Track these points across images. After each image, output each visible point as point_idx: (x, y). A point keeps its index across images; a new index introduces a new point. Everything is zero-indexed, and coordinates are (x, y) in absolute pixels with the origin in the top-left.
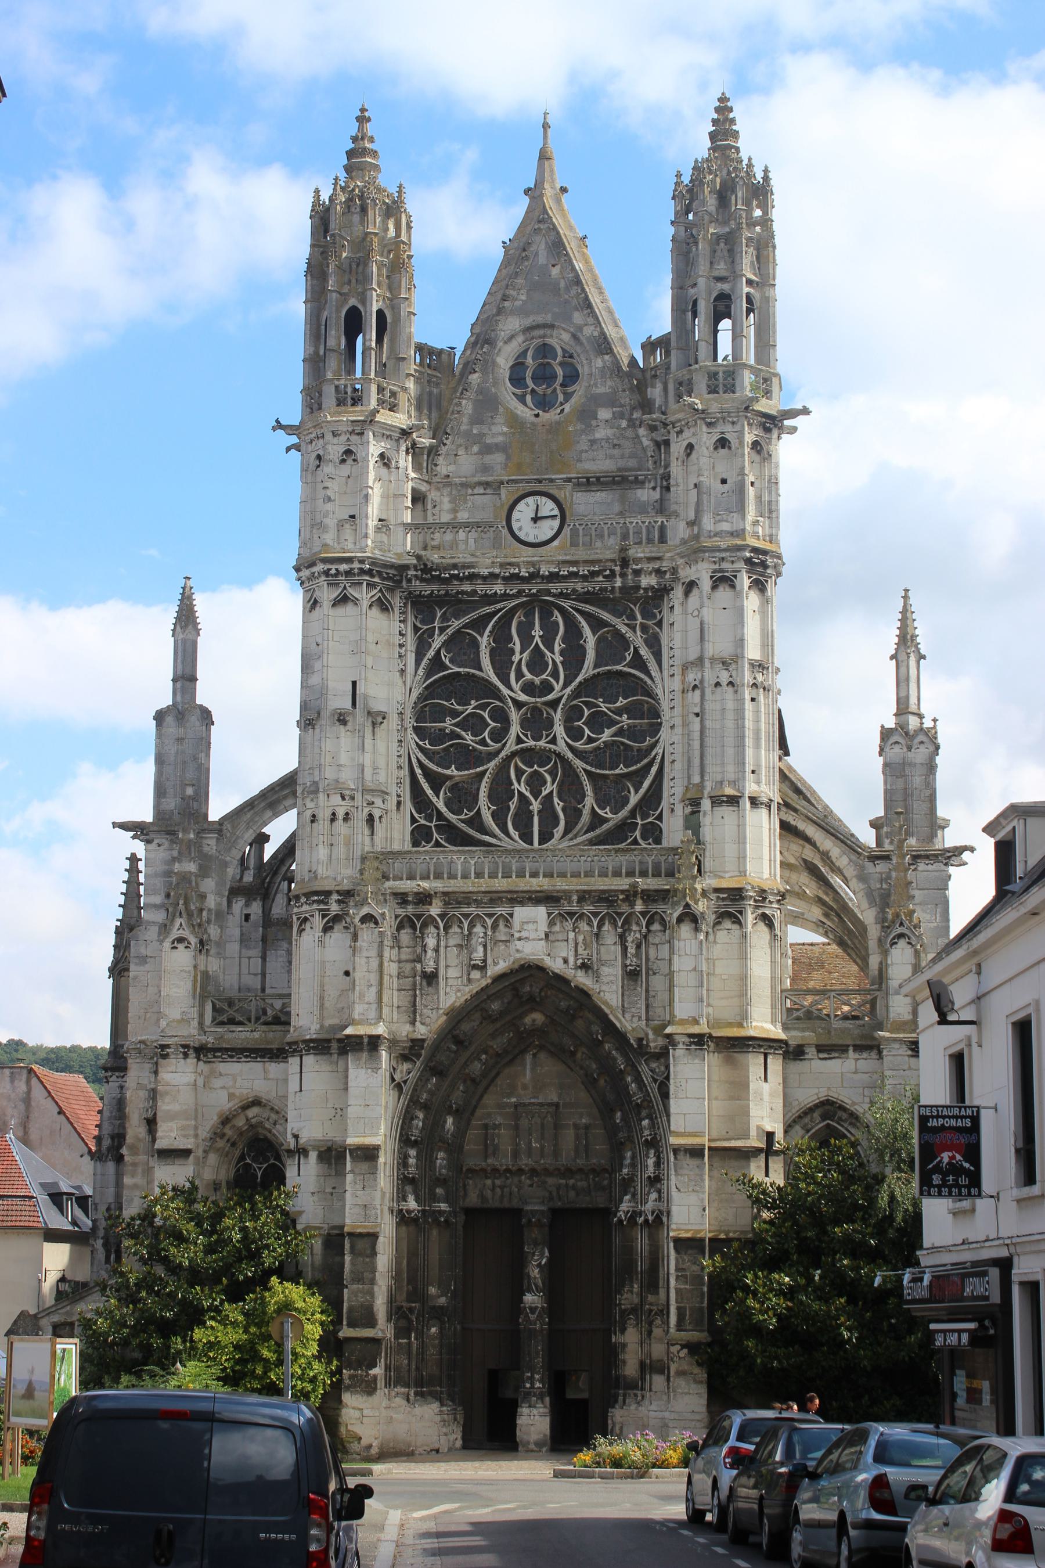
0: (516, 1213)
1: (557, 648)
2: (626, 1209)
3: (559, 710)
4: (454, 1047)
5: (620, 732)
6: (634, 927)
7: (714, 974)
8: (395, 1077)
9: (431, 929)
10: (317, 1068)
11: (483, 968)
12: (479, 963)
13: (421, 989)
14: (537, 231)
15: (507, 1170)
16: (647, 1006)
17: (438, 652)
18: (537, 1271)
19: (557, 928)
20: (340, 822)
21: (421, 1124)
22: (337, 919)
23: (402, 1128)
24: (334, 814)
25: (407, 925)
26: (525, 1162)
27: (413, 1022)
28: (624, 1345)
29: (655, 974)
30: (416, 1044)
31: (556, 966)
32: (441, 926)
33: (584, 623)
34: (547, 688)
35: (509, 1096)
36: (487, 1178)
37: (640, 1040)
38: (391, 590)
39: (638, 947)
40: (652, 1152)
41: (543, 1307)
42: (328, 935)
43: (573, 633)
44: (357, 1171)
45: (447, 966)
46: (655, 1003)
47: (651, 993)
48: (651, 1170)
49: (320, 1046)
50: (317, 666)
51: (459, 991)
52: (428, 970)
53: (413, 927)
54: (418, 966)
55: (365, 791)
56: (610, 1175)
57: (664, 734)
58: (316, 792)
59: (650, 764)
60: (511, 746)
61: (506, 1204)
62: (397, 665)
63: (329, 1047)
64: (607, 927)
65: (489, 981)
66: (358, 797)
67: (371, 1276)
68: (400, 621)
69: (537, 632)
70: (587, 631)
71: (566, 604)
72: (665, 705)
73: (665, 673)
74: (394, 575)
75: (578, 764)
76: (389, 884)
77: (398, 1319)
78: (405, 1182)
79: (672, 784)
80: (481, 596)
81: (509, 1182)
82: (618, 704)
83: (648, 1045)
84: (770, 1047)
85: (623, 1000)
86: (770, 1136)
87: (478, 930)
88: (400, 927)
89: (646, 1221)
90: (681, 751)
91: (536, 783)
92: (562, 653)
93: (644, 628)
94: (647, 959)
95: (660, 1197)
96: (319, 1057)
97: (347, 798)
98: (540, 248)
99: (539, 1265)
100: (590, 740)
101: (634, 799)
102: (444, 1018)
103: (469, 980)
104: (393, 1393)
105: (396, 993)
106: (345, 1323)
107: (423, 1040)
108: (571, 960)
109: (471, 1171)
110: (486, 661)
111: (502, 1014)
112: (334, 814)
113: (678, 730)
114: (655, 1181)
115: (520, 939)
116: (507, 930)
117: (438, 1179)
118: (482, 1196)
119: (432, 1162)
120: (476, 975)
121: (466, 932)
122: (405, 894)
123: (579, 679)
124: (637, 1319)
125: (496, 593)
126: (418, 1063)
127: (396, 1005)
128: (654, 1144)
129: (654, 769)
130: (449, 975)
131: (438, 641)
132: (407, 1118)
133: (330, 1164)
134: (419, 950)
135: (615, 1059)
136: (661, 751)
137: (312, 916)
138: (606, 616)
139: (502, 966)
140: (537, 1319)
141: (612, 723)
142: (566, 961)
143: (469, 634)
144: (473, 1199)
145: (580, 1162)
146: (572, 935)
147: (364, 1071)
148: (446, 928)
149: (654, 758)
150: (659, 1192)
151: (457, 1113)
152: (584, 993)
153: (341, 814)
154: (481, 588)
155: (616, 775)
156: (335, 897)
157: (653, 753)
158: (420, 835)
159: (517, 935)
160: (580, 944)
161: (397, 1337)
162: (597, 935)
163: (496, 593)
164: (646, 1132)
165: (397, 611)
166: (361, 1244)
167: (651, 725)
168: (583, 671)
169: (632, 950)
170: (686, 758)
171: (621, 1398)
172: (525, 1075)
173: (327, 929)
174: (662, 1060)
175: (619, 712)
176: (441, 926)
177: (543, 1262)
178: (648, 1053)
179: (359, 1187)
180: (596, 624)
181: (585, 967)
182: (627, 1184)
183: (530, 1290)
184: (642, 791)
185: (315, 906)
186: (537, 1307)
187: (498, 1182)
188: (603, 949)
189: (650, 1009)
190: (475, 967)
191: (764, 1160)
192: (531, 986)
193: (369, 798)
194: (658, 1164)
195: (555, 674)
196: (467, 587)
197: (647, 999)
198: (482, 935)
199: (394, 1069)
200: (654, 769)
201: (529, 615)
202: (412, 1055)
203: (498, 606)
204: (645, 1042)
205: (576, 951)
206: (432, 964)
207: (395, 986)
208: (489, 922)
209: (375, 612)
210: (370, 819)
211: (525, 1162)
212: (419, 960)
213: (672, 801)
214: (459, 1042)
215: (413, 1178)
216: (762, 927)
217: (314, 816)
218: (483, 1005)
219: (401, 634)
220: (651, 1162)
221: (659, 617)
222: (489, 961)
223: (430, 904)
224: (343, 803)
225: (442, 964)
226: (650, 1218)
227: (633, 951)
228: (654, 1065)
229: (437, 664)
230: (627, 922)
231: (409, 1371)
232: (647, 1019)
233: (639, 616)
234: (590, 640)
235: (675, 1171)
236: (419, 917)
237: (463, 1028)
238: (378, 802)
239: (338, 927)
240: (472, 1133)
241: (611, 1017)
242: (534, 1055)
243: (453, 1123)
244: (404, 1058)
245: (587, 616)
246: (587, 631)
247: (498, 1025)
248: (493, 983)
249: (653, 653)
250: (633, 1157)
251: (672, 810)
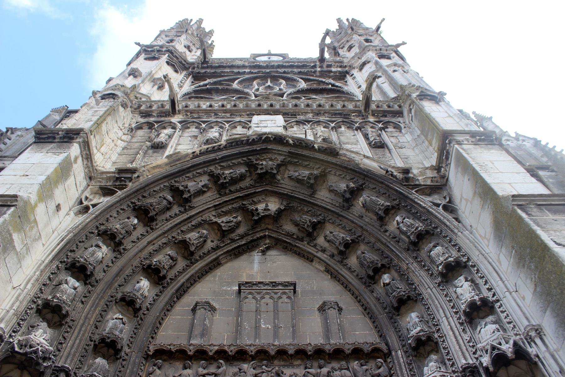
15: (222, 354)
35: (230, 284)
36: (185, 368)
37: (406, 171)
145: (336, 341)
172: (252, 268)
202: (115, 186)
226: (507, 348)
235: (538, 225)
242: (264, 252)
244: (106, 191)
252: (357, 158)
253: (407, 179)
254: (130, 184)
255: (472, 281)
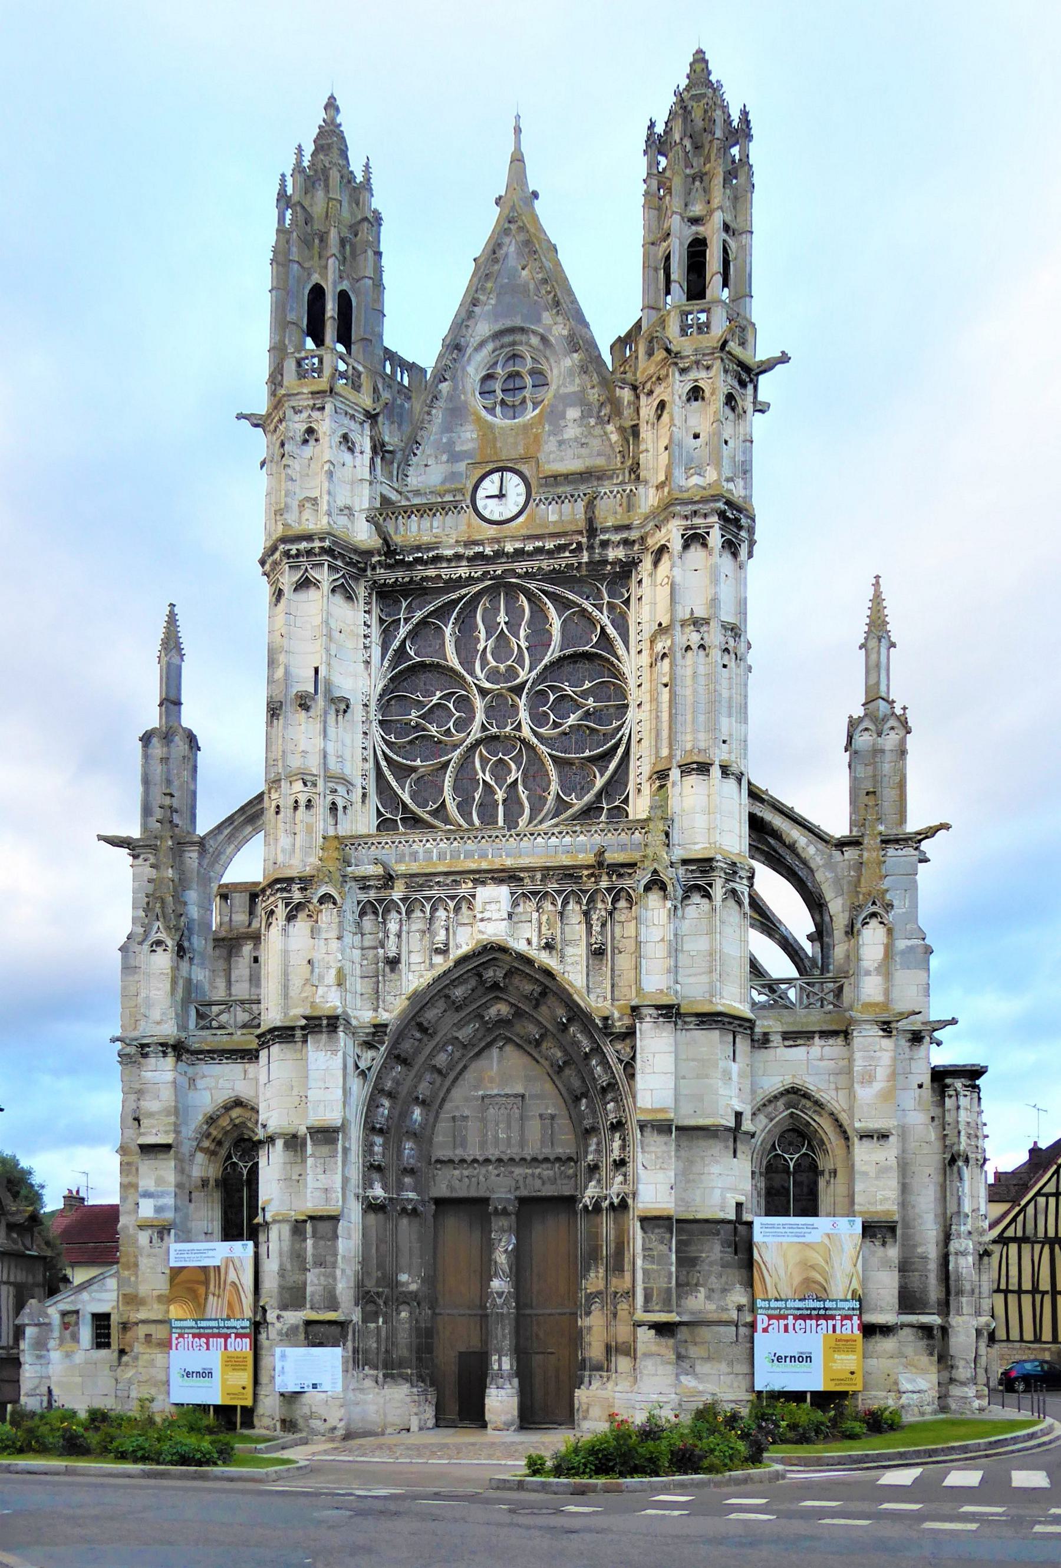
0: (485, 1201)
1: (522, 634)
2: (591, 1195)
3: (524, 695)
4: (418, 1035)
5: (587, 715)
6: (600, 905)
7: (682, 950)
8: (359, 1065)
9: (394, 915)
10: (282, 1056)
11: (444, 951)
12: (441, 946)
13: (384, 976)
14: (507, 232)
16: (613, 986)
17: (404, 642)
18: (504, 1256)
19: (520, 909)
20: (302, 808)
21: (386, 1112)
22: (299, 907)
23: (366, 1117)
24: (296, 802)
25: (369, 910)
26: (491, 1151)
27: (376, 1010)
28: (590, 1328)
29: (620, 952)
30: (379, 1028)
31: (521, 946)
32: (403, 910)
33: (549, 604)
34: (512, 673)
36: (455, 1169)
37: (606, 1019)
38: (356, 579)
39: (604, 925)
40: (617, 1135)
41: (509, 1292)
42: (291, 924)
43: (540, 614)
44: (317, 1154)
45: (410, 952)
46: (621, 982)
47: (617, 973)
48: (616, 1154)
49: (284, 1034)
50: (282, 658)
51: (422, 976)
52: (391, 955)
53: (375, 913)
54: (381, 951)
55: (329, 777)
56: (576, 1163)
57: (632, 714)
58: (280, 780)
59: (616, 746)
60: (475, 732)
61: (473, 1193)
62: (360, 656)
63: (293, 1036)
64: (570, 907)
65: (451, 964)
66: (320, 783)
67: (332, 1259)
68: (365, 612)
69: (502, 618)
70: (552, 612)
71: (532, 586)
72: (632, 682)
73: (633, 651)
74: (359, 562)
75: (543, 749)
76: (349, 869)
77: (367, 1303)
78: (373, 1168)
79: (638, 763)
80: (446, 582)
81: (476, 1172)
82: (585, 687)
83: (613, 1025)
84: (740, 1026)
85: (588, 980)
86: (738, 1115)
87: (441, 914)
88: (362, 914)
89: (612, 1204)
90: (648, 728)
91: (500, 769)
92: (527, 638)
93: (611, 607)
94: (613, 938)
95: (625, 1180)
96: (283, 1046)
97: (309, 784)
98: (511, 248)
99: (506, 1251)
100: (556, 725)
101: (599, 782)
102: (407, 1002)
103: (432, 965)
104: (361, 1375)
105: (359, 980)
106: (308, 1306)
107: (386, 1026)
108: (535, 941)
109: (438, 1161)
110: (450, 649)
111: (466, 1001)
112: (296, 802)
113: (646, 707)
114: (621, 1164)
115: (482, 920)
116: (470, 912)
117: (405, 1169)
118: (451, 1187)
119: (400, 1151)
120: (438, 959)
121: (428, 915)
122: (365, 878)
123: (544, 662)
124: (602, 1301)
125: (460, 576)
126: (382, 1049)
127: (359, 992)
128: (618, 1126)
129: (620, 751)
130: (412, 961)
131: (403, 631)
132: (372, 1104)
133: (296, 1151)
134: (381, 935)
135: (580, 1042)
136: (628, 731)
137: (276, 907)
138: (572, 596)
139: (465, 949)
140: (504, 1304)
141: (579, 706)
142: (529, 942)
143: (434, 624)
144: (441, 1190)
146: (535, 915)
147: (323, 1053)
148: (409, 912)
149: (621, 739)
150: (625, 1175)
151: (423, 1103)
152: (549, 973)
153: (302, 802)
154: (445, 573)
155: (582, 758)
156: (295, 887)
157: (621, 733)
158: (385, 825)
159: (479, 916)
160: (544, 924)
161: (365, 1320)
162: (561, 914)
163: (460, 576)
164: (612, 1116)
165: (362, 601)
166: (323, 1226)
167: (618, 707)
168: (549, 654)
169: (596, 928)
170: (653, 735)
171: (586, 1380)
173: (290, 918)
174: (628, 1041)
175: (584, 694)
176: (403, 910)
177: (510, 1248)
178: (612, 1034)
179: (320, 1170)
180: (563, 604)
181: (549, 947)
182: (594, 1168)
183: (496, 1275)
184: (608, 774)
185: (279, 895)
186: (503, 1293)
187: (466, 1173)
188: (567, 928)
189: (616, 989)
190: (438, 951)
191: (732, 1140)
192: (495, 971)
193: (330, 785)
194: (623, 1147)
195: (520, 660)
196: (432, 573)
197: (612, 978)
198: (444, 918)
199: (358, 1056)
200: (620, 751)
201: (494, 600)
203: (463, 592)
204: (610, 1022)
205: (540, 931)
206: (394, 948)
207: (358, 972)
208: (451, 905)
209: (338, 599)
210: (334, 808)
211: (493, 1153)
212: (383, 947)
213: (639, 781)
214: (422, 1029)
215: (379, 1165)
216: (731, 903)
217: (278, 807)
218: (447, 991)
219: (365, 624)
220: (617, 1144)
221: (626, 596)
222: (451, 945)
223: (392, 888)
224: (305, 789)
225: (404, 949)
226: (616, 1201)
227: (598, 929)
228: (619, 1047)
229: (401, 651)
230: (591, 900)
231: (377, 1354)
232: (613, 999)
233: (606, 596)
234: (556, 623)
236: (380, 901)
237: (426, 1015)
238: (342, 790)
239: (302, 916)
240: (443, 1126)
241: (576, 997)
243: (421, 1114)
244: (369, 1045)
245: (553, 597)
246: (552, 612)
247: (463, 1014)
248: (455, 966)
249: (619, 634)
250: (598, 1144)
251: (639, 790)
252: (571, 991)
253: (606, 1027)
254: (386, 1038)
255: (624, 1140)
